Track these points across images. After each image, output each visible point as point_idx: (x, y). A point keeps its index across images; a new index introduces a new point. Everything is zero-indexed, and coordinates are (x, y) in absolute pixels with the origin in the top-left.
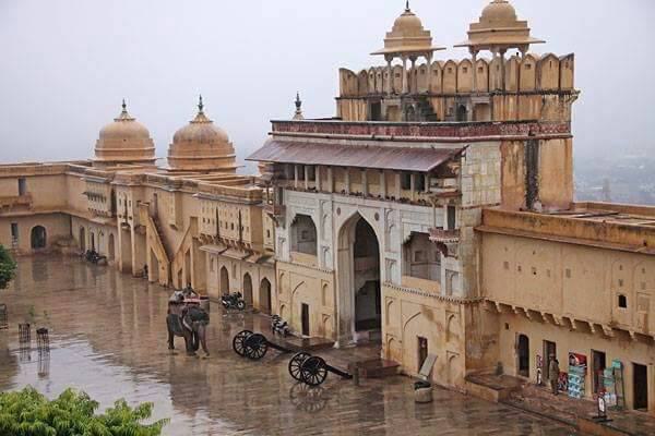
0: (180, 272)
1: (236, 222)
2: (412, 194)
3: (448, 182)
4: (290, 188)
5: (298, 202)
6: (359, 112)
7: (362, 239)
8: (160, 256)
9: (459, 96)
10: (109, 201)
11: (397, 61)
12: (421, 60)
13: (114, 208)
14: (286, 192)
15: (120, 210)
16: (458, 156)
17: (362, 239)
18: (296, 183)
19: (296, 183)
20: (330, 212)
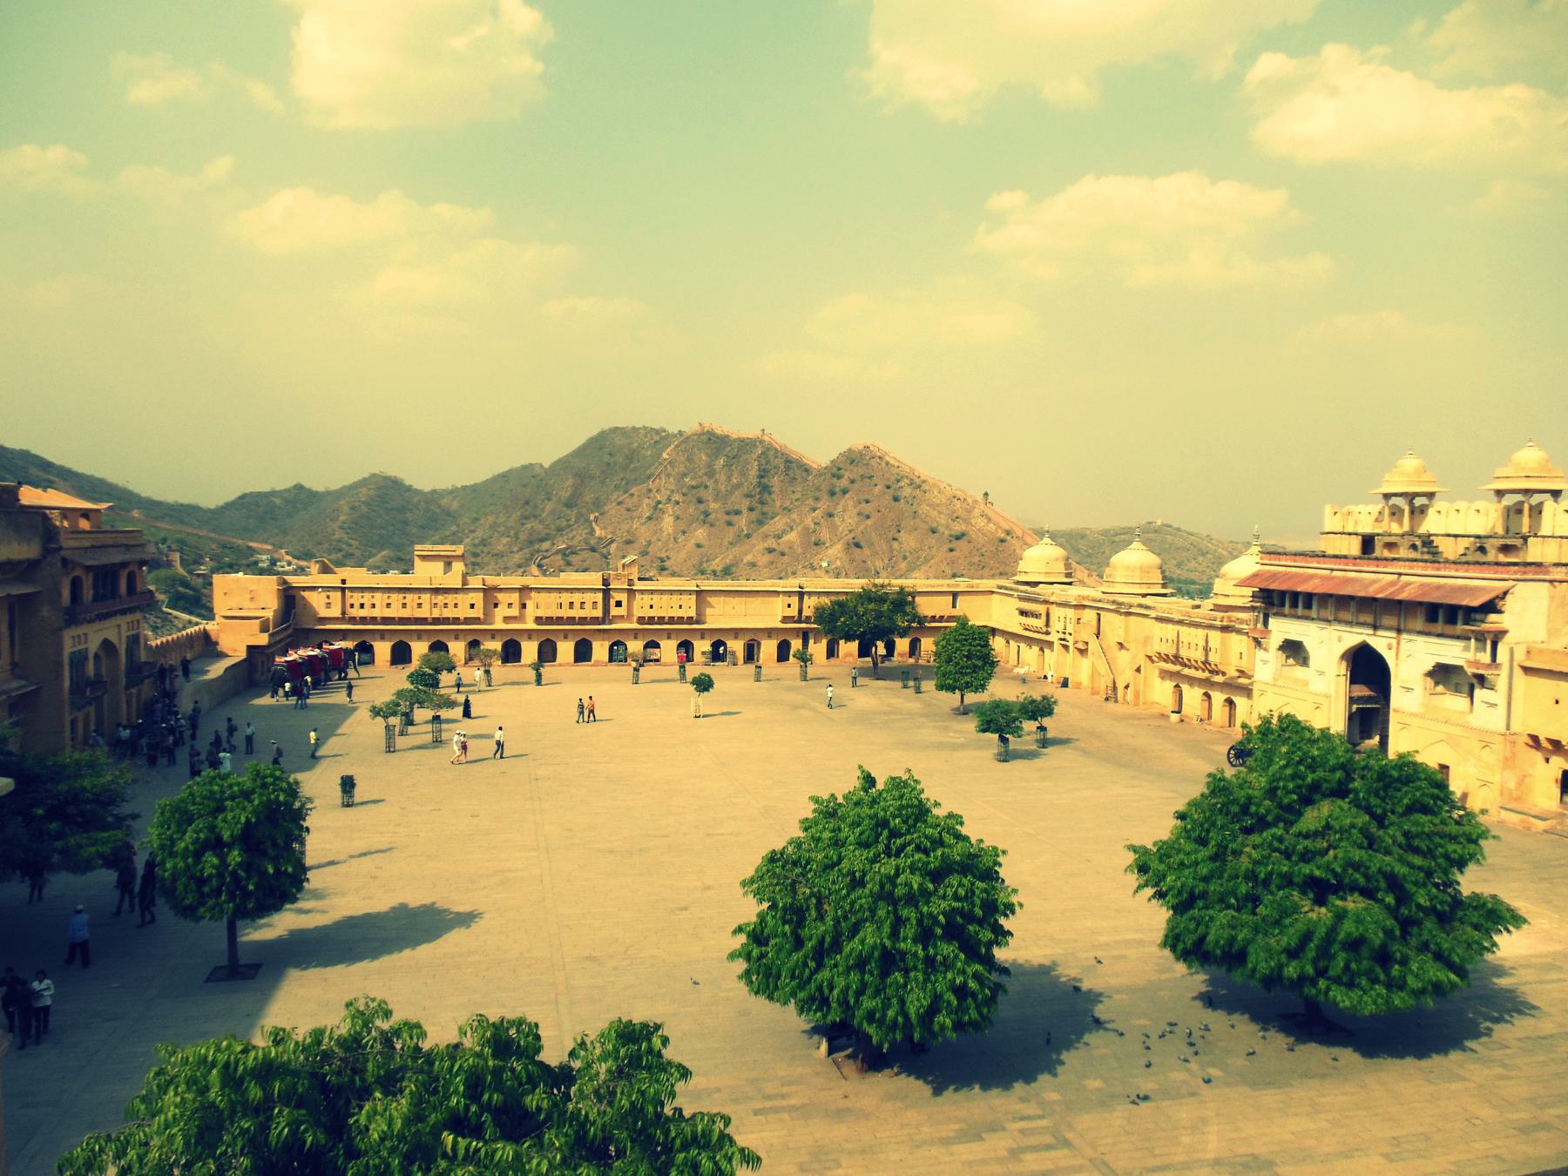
0: (1127, 687)
1: (1202, 643)
2: (1439, 627)
3: (1493, 617)
4: (1276, 614)
5: (1282, 628)
6: (1354, 547)
7: (1367, 669)
8: (1103, 668)
9: (1478, 537)
10: (1044, 618)
11: (1394, 500)
12: (1418, 502)
13: (1047, 625)
14: (1272, 621)
15: (1056, 625)
16: (1506, 593)
17: (1367, 669)
18: (1287, 609)
19: (1287, 609)
20: (1328, 643)
